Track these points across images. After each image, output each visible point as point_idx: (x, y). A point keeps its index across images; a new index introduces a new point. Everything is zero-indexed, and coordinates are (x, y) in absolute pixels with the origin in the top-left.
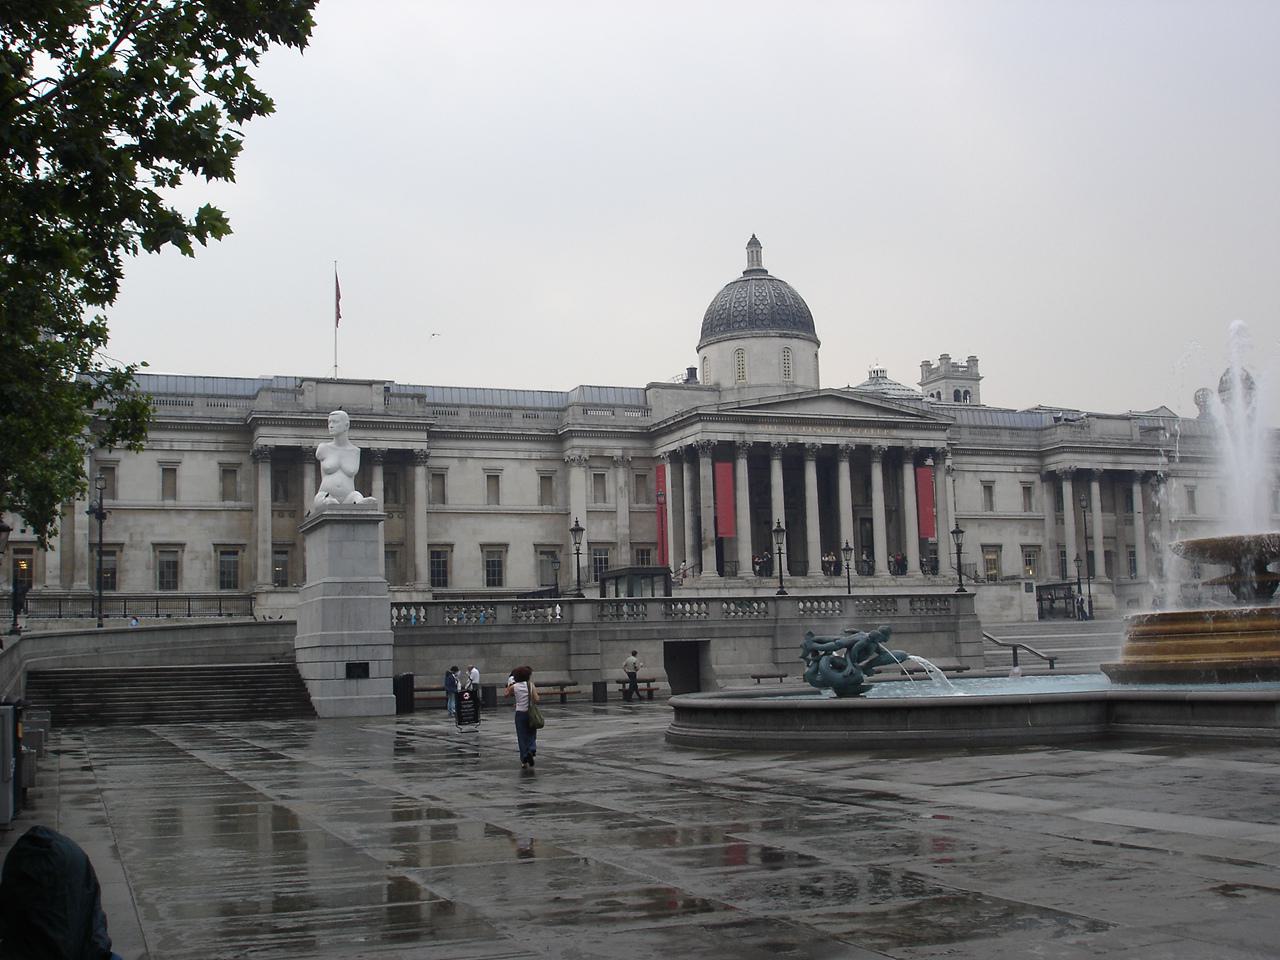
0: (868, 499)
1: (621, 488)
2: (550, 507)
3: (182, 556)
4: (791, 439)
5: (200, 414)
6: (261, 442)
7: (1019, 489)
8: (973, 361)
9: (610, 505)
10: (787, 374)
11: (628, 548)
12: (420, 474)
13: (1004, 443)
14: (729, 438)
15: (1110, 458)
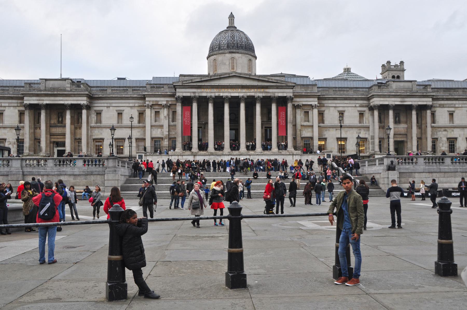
0: (270, 119)
1: (165, 117)
2: (142, 124)
3: (5, 143)
4: (217, 94)
5: (11, 93)
6: (25, 102)
7: (357, 114)
8: (402, 63)
9: (161, 123)
10: (233, 68)
11: (168, 140)
12: (84, 112)
13: (350, 94)
14: (188, 95)
15: (399, 99)
